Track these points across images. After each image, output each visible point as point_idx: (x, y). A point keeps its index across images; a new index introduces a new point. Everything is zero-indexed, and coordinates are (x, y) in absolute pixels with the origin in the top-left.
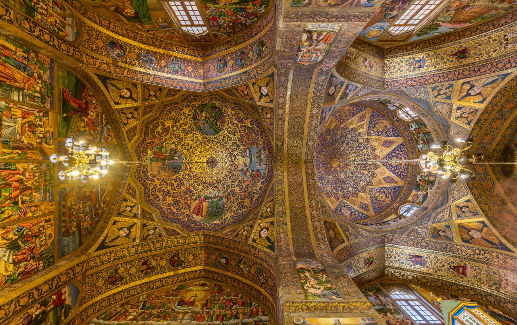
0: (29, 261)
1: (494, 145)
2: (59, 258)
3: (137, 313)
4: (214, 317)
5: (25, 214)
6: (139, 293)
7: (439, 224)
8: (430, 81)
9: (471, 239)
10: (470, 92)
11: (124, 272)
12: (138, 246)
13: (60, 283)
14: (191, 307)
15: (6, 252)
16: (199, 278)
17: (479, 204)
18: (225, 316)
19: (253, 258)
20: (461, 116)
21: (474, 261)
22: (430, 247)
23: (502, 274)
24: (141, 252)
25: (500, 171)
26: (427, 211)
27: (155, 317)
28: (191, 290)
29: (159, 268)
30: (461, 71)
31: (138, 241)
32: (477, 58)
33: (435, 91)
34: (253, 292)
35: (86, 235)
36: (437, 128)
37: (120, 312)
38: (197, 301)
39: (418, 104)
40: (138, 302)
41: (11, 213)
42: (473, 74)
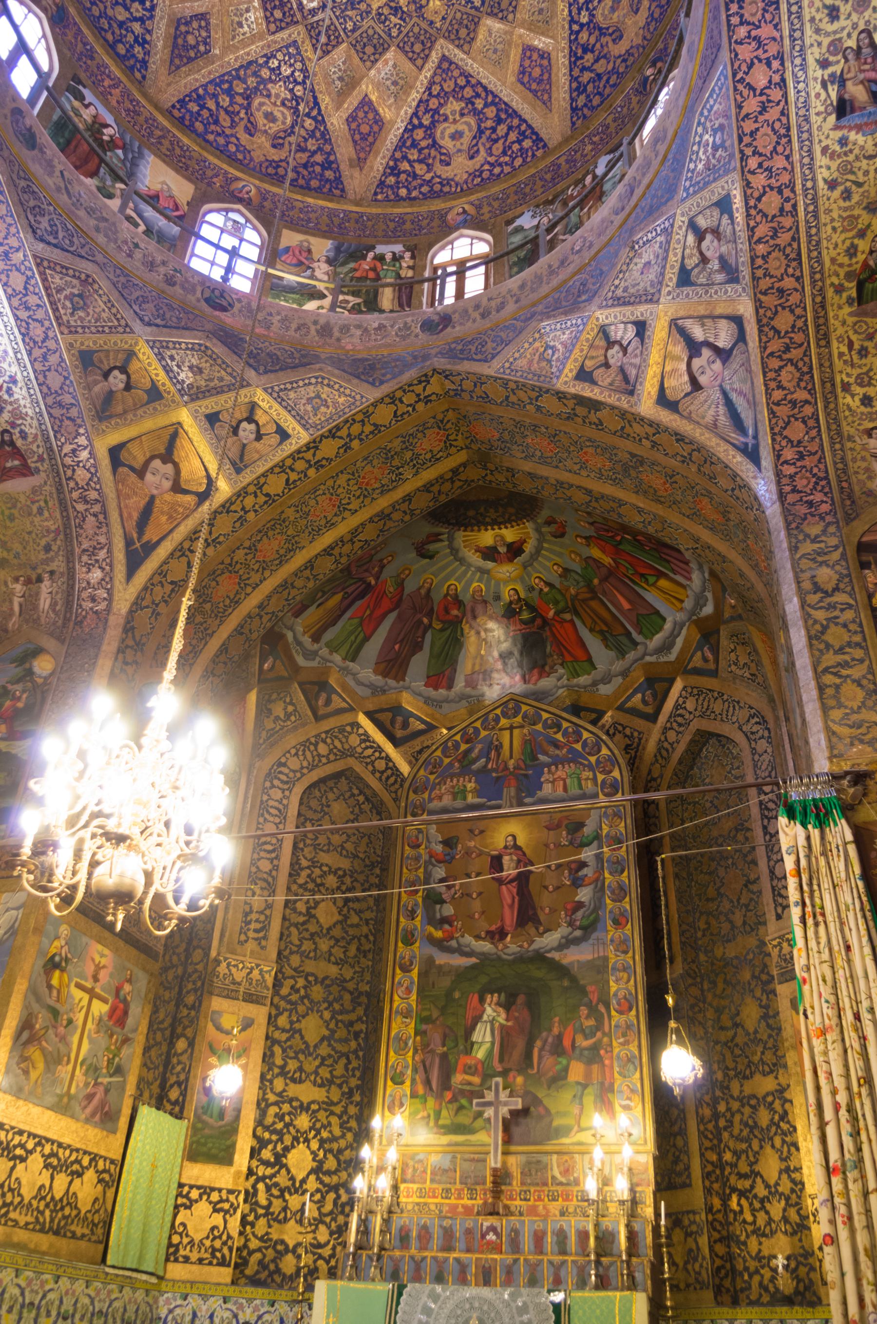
1: (528, 466)
7: (155, 364)
8: (759, 181)
9: (132, 469)
10: (706, 353)
17: (281, 467)
20: (610, 344)
21: (60, 490)
22: (37, 352)
23: (53, 566)
25: (443, 499)
26: (208, 310)
30: (794, 298)
32: (851, 345)
33: (716, 213)
36: (571, 269)
39: (670, 156)
42: (775, 346)
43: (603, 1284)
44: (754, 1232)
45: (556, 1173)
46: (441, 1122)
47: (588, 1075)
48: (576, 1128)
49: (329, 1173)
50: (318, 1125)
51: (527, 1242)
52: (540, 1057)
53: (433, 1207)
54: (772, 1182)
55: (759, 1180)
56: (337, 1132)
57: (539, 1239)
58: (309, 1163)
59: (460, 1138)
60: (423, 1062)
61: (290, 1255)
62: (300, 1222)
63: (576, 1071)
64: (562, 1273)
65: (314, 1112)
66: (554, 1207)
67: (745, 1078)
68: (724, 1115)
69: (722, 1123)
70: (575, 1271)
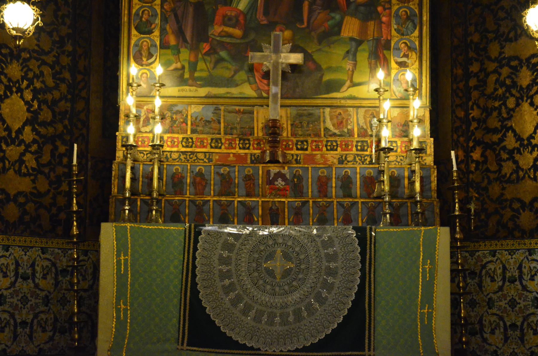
43: (396, 221)
44: (496, 179)
45: (329, 124)
46: (197, 74)
47: (363, 31)
48: (348, 83)
49: (44, 124)
50: (30, 75)
51: (310, 188)
52: (311, 12)
53: (201, 156)
54: (526, 136)
55: (510, 134)
56: (50, 82)
57: (323, 185)
58: (24, 115)
59: (221, 91)
60: (174, 11)
61: (12, 204)
62: (19, 172)
63: (351, 27)
64: (353, 213)
65: (26, 60)
66: (332, 157)
67: (509, 40)
68: (476, 75)
69: (473, 82)
70: (365, 212)
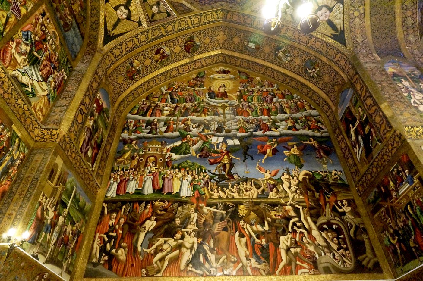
0: (54, 73)
2: (74, 60)
3: (170, 107)
4: (258, 111)
5: (19, 11)
6: (157, 84)
11: (139, 65)
12: (147, 31)
13: (94, 91)
14: (226, 100)
15: (31, 71)
16: (216, 63)
18: (269, 110)
19: (303, 48)
24: (152, 40)
27: (193, 112)
28: (214, 79)
29: (174, 56)
31: (144, 24)
34: (293, 84)
35: (82, 22)
37: (150, 106)
38: (229, 92)
40: (162, 94)
41: (5, 15)
